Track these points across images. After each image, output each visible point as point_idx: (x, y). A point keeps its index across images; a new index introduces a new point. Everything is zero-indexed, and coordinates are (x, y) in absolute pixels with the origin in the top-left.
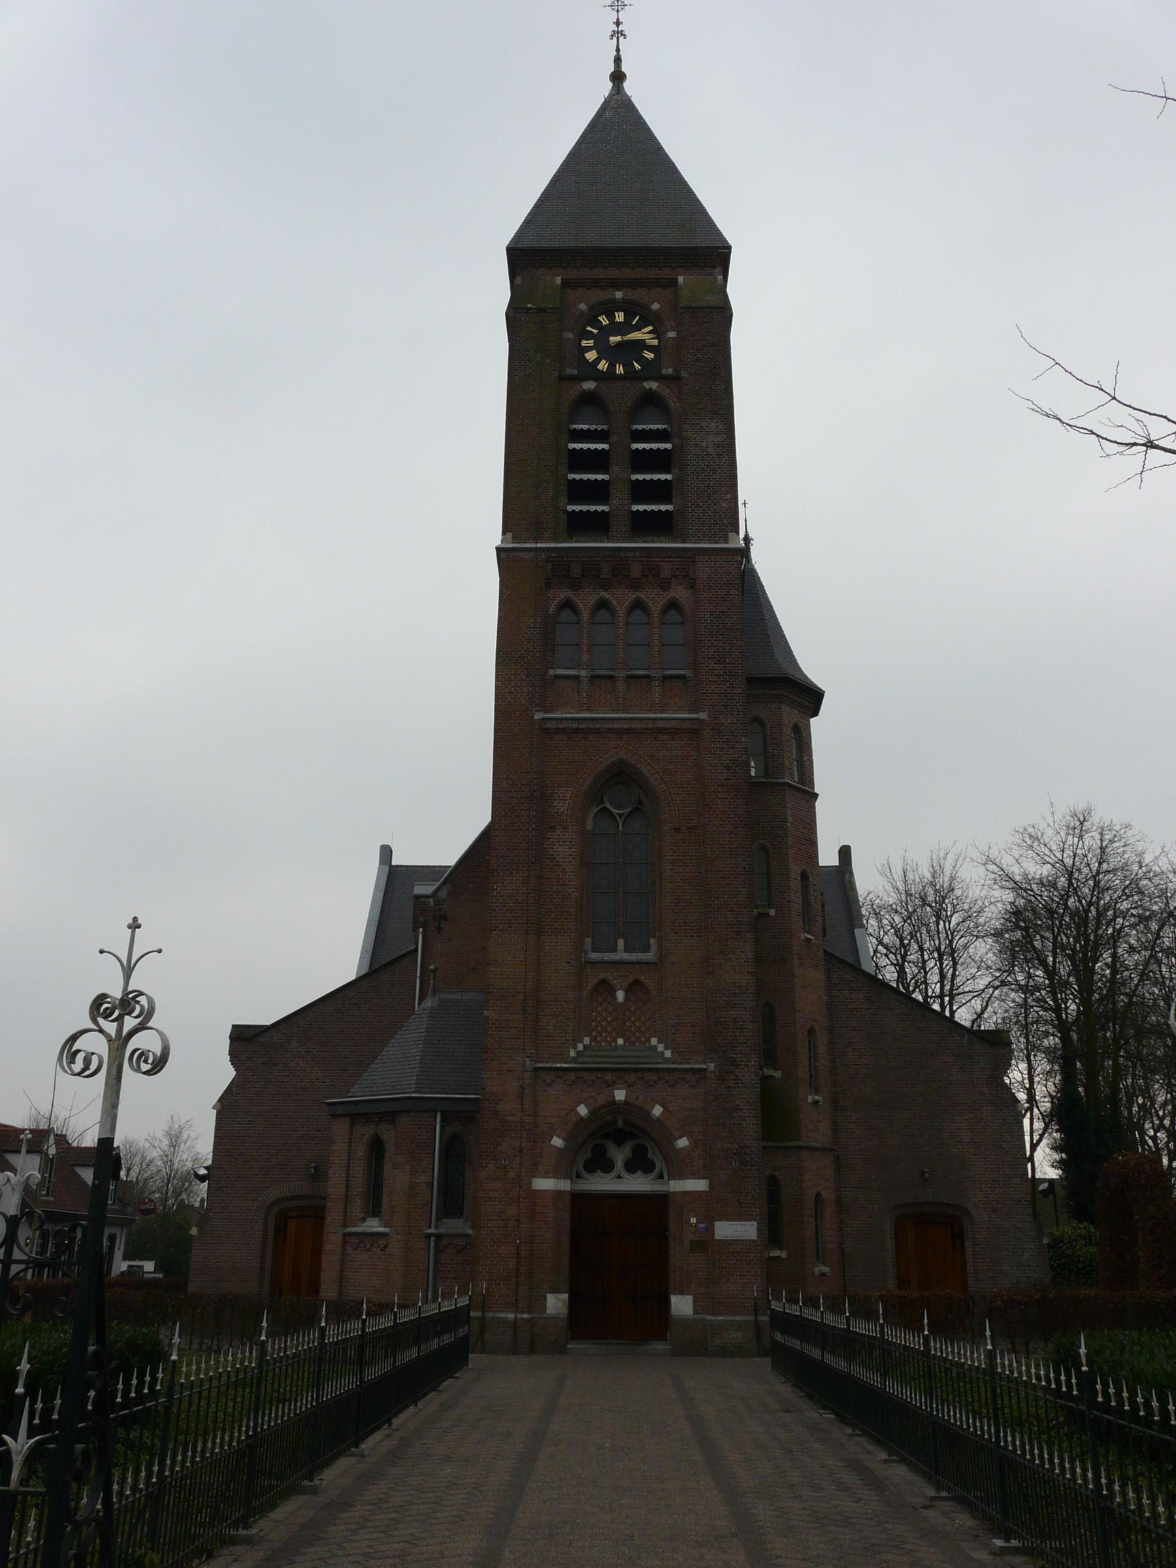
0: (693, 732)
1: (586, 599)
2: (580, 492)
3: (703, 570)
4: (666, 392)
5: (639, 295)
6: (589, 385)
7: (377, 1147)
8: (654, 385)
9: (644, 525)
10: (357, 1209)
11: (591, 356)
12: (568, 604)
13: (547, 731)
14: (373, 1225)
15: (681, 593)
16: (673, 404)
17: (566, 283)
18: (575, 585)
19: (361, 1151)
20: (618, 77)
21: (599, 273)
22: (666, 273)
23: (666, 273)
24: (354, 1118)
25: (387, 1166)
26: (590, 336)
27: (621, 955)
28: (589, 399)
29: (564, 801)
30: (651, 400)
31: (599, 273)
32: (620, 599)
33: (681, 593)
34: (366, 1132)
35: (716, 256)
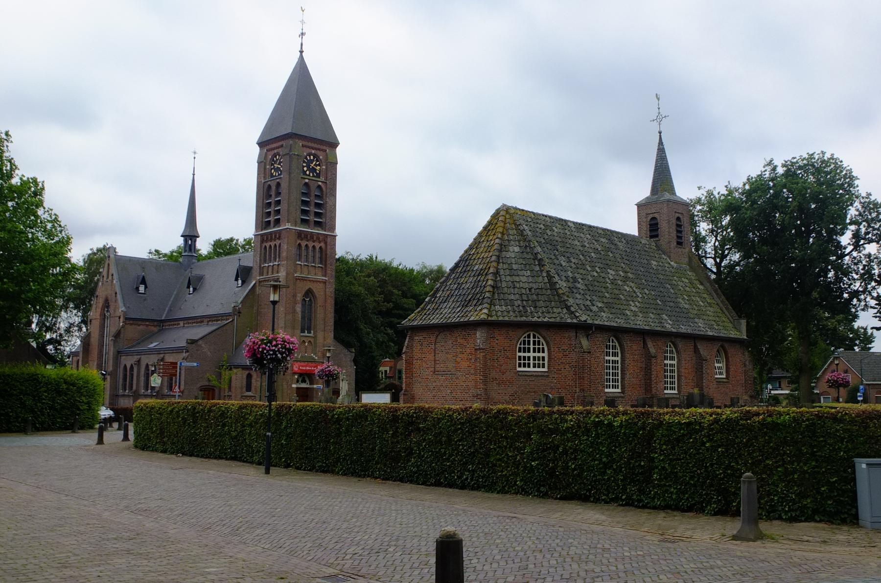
0: (325, 282)
1: (304, 243)
2: (304, 212)
3: (329, 240)
4: (323, 186)
5: (318, 153)
6: (307, 181)
7: (249, 377)
8: (320, 183)
9: (318, 224)
10: (244, 390)
11: (305, 169)
12: (300, 245)
13: (297, 279)
14: (249, 394)
15: (322, 244)
16: (324, 189)
17: (303, 146)
18: (302, 240)
19: (245, 377)
20: (301, 52)
21: (310, 144)
22: (324, 148)
23: (324, 148)
24: (243, 369)
25: (253, 381)
26: (304, 162)
27: (306, 334)
28: (306, 184)
29: (299, 297)
30: (319, 186)
31: (310, 144)
32: (311, 244)
33: (322, 244)
34: (247, 372)
35: (334, 144)
